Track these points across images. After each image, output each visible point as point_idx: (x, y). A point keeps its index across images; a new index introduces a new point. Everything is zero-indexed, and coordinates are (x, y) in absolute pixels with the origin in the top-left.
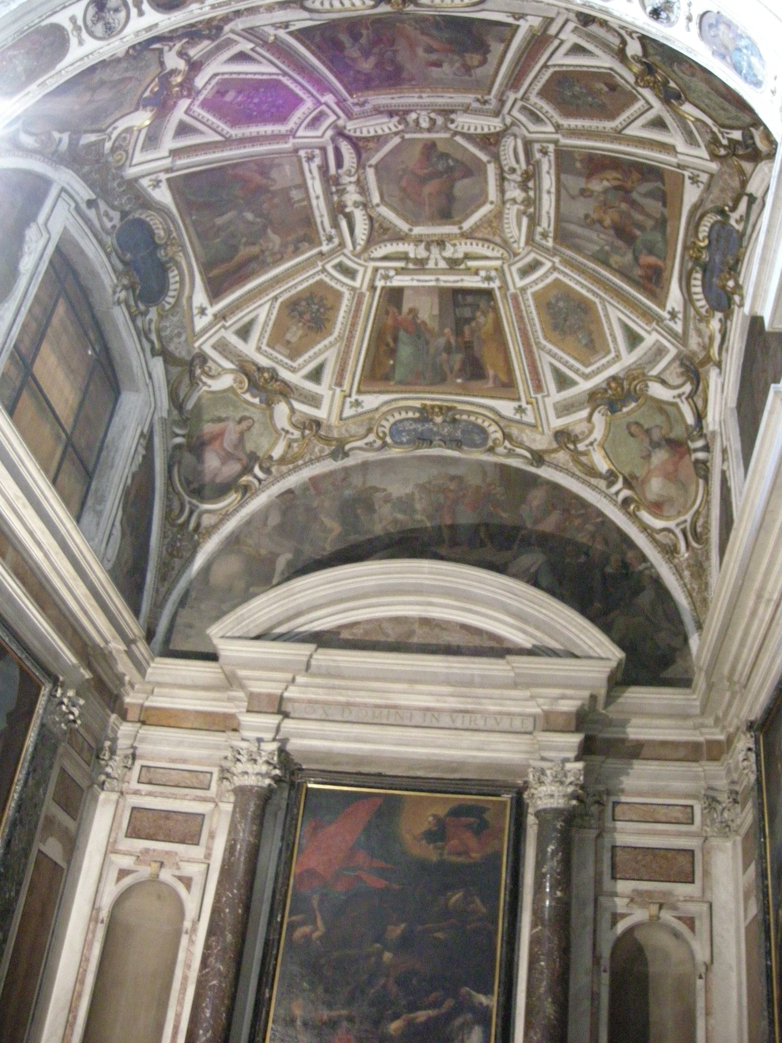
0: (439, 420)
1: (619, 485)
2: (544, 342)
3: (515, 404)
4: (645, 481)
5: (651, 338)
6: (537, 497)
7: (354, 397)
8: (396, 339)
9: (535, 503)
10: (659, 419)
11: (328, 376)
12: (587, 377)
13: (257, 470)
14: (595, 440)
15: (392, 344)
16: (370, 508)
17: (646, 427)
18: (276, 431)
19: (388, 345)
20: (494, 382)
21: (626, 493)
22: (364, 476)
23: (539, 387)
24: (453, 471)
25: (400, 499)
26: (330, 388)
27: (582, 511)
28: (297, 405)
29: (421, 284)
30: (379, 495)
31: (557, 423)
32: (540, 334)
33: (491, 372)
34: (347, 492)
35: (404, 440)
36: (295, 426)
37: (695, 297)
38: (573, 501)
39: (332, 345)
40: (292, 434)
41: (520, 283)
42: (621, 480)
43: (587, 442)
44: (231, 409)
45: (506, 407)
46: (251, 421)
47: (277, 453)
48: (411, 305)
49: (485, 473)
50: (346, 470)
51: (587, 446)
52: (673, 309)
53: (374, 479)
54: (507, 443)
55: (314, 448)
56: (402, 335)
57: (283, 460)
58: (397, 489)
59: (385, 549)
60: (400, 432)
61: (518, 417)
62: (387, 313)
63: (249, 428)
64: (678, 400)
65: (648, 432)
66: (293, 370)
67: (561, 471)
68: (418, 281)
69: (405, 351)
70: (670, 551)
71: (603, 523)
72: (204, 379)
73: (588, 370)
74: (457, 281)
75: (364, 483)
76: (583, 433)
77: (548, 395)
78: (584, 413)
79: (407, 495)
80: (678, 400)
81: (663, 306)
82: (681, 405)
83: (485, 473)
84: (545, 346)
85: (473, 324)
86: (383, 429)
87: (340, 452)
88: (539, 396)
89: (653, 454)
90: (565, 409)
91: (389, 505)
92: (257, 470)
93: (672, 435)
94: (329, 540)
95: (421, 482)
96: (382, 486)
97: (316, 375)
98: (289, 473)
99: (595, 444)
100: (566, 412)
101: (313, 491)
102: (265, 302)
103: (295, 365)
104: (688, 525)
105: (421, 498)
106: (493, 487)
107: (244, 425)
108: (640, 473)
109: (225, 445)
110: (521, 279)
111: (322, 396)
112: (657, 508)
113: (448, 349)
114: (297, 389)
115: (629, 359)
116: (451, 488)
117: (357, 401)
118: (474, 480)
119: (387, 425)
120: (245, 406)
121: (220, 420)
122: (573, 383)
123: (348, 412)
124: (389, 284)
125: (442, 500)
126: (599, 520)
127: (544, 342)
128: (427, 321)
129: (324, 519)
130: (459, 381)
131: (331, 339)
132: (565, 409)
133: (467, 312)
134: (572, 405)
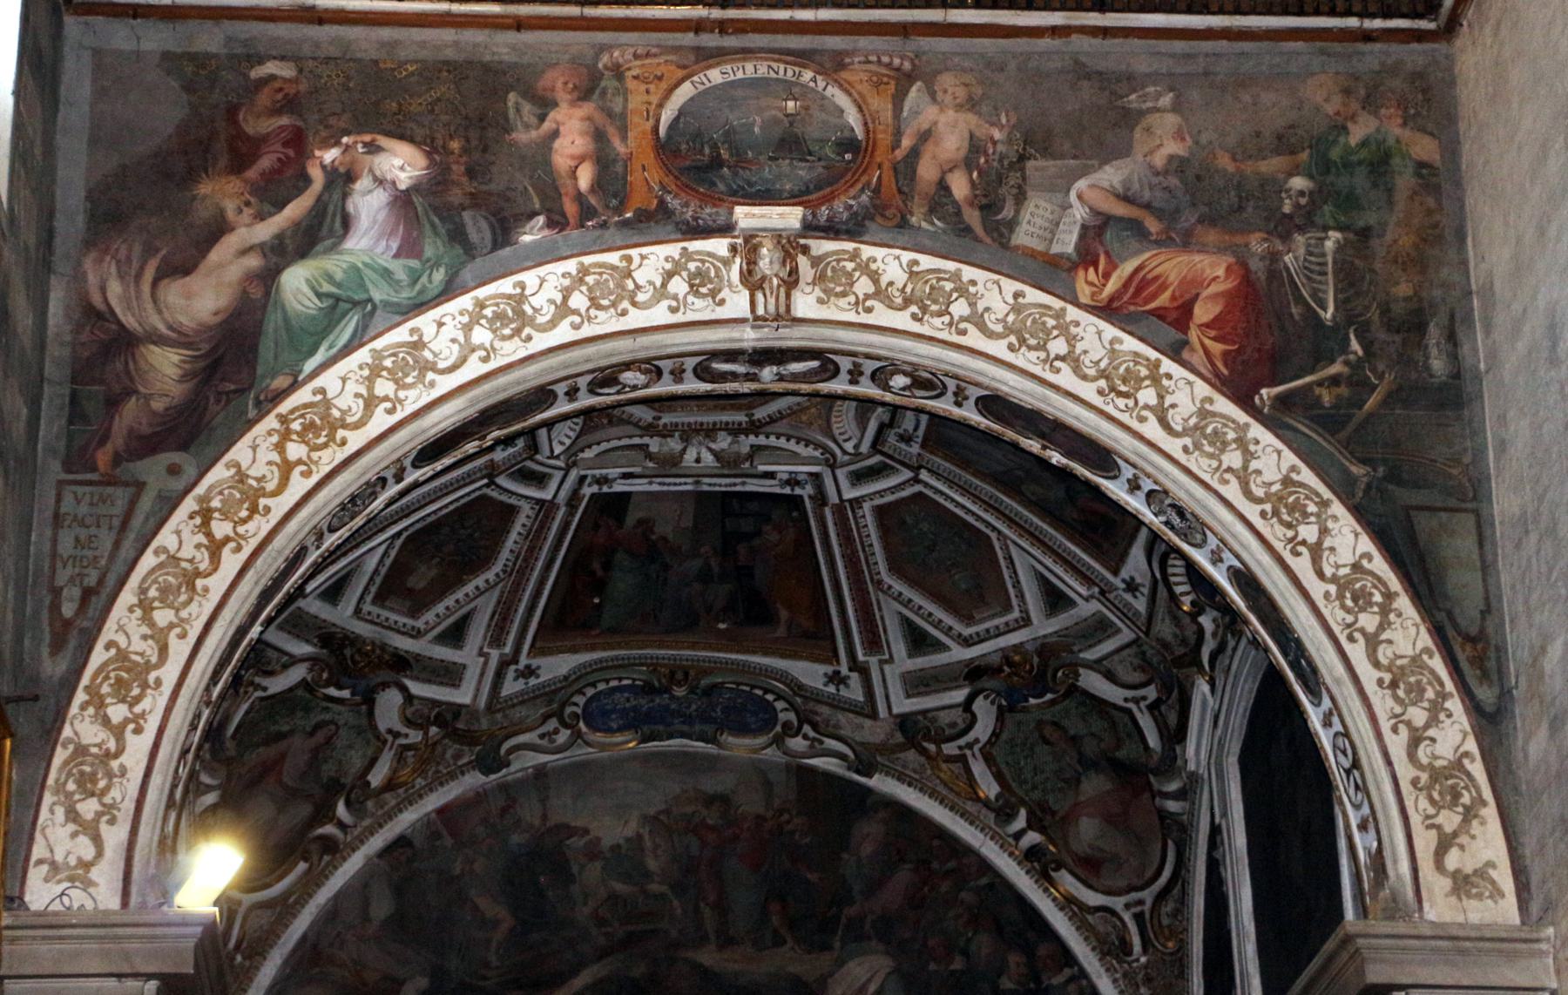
0: (680, 692)
1: (1020, 822)
2: (888, 579)
3: (829, 669)
4: (1068, 819)
5: (1087, 608)
6: (869, 835)
7: (524, 661)
8: (607, 566)
9: (867, 849)
10: (1097, 725)
11: (477, 633)
12: (967, 642)
13: (341, 810)
14: (977, 741)
15: (600, 573)
16: (562, 871)
17: (1072, 732)
18: (378, 737)
19: (593, 573)
20: (789, 628)
21: (1033, 837)
22: (543, 801)
23: (874, 642)
24: (710, 785)
25: (616, 848)
26: (481, 653)
27: (951, 865)
28: (416, 688)
29: (665, 488)
30: (577, 842)
31: (904, 705)
32: (882, 567)
33: (784, 614)
34: (516, 839)
35: (614, 725)
36: (409, 722)
37: (1173, 579)
38: (936, 843)
39: (490, 587)
40: (406, 736)
41: (849, 494)
42: (1023, 812)
43: (962, 742)
44: (299, 714)
45: (811, 674)
46: (333, 727)
47: (376, 778)
48: (641, 514)
49: (768, 785)
50: (504, 787)
51: (960, 748)
52: (1132, 579)
53: (564, 808)
54: (807, 729)
55: (444, 753)
56: (620, 557)
57: (390, 785)
58: (612, 830)
59: (600, 958)
60: (605, 714)
61: (831, 689)
62: (597, 526)
63: (328, 741)
64: (1131, 705)
65: (1074, 740)
66: (417, 634)
67: (910, 785)
68: (660, 484)
69: (623, 582)
70: (1113, 949)
71: (991, 886)
72: (257, 680)
73: (968, 631)
74: (735, 485)
75: (544, 817)
76: (953, 725)
77: (891, 660)
78: (959, 695)
79: (628, 840)
80: (1131, 705)
81: (1116, 573)
82: (1138, 715)
83: (768, 785)
84: (890, 587)
85: (756, 542)
86: (575, 709)
87: (492, 762)
88: (873, 661)
89: (1083, 778)
90: (918, 683)
91: (598, 865)
92: (341, 810)
93: (1121, 754)
94: (494, 944)
95: (652, 811)
96: (579, 823)
97: (455, 635)
98: (399, 809)
99: (976, 748)
100: (922, 689)
101: (448, 841)
102: (380, 544)
103: (420, 624)
104: (1147, 907)
105: (656, 847)
106: (786, 817)
107: (320, 737)
108: (1060, 804)
109: (286, 779)
110: (853, 485)
111: (464, 667)
112: (1090, 868)
113: (705, 577)
114: (418, 661)
115: (1044, 627)
116: (710, 822)
117: (528, 667)
118: (751, 804)
119: (581, 700)
120: (325, 704)
121: (281, 736)
122: (940, 647)
123: (511, 687)
124: (605, 489)
125: (695, 851)
126: (984, 881)
127: (888, 579)
128: (670, 537)
129: (479, 901)
130: (722, 626)
131: (490, 575)
132: (918, 683)
133: (747, 525)
134: (936, 679)
